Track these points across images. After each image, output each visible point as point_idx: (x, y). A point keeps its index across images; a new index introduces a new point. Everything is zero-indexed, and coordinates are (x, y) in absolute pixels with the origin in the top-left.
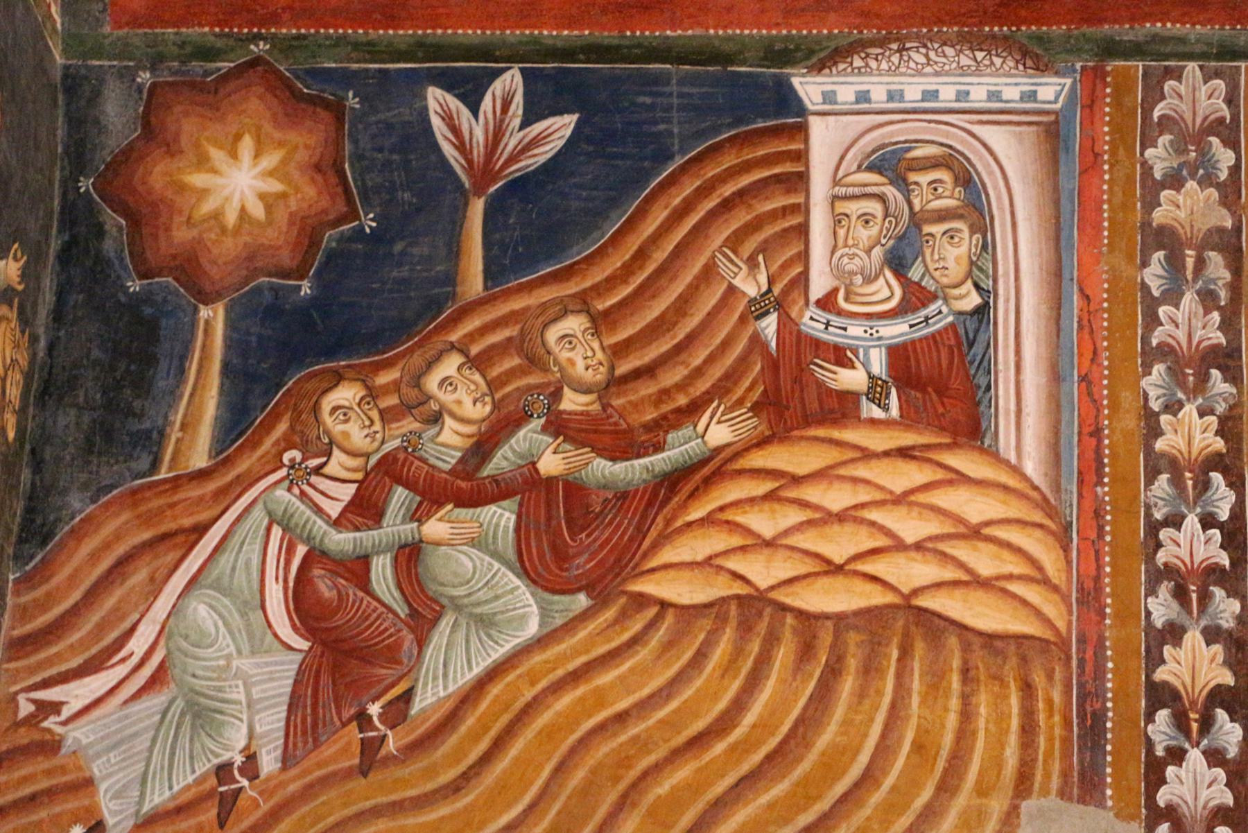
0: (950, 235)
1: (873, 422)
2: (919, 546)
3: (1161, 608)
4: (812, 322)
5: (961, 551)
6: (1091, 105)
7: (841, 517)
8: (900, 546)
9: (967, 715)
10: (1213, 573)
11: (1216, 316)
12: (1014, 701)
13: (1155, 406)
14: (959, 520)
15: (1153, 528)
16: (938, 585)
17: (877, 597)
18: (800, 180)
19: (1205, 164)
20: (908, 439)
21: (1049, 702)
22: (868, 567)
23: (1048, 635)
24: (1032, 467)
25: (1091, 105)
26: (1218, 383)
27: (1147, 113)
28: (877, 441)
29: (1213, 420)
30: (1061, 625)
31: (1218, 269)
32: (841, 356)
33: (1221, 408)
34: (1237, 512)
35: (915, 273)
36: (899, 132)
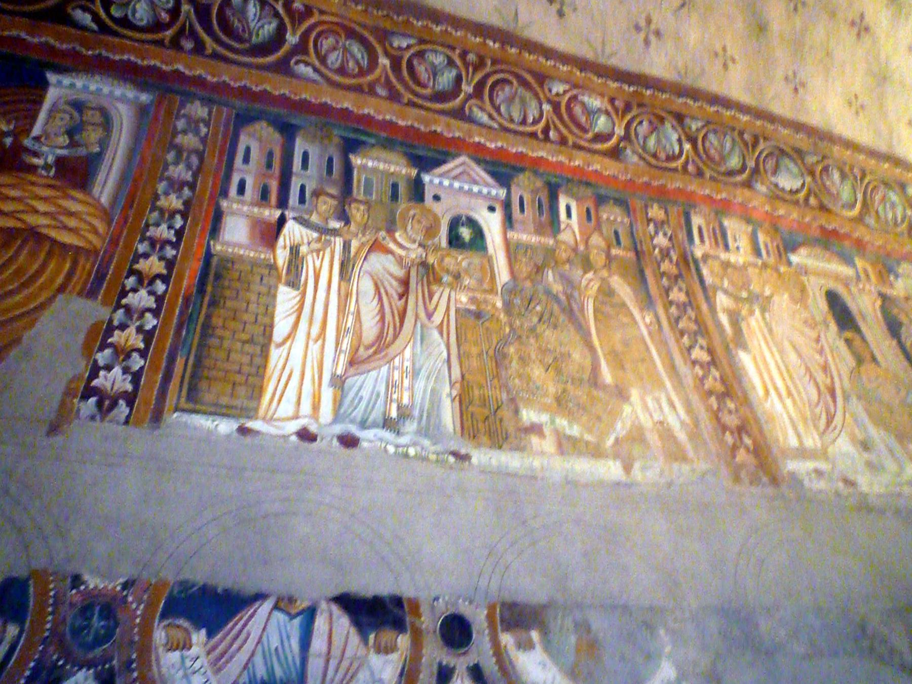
0: (94, 130)
1: (42, 176)
2: (45, 214)
3: (142, 248)
4: (27, 142)
5: (64, 219)
6: (159, 104)
7: (14, 199)
8: (36, 211)
9: (44, 266)
10: (169, 242)
11: (190, 173)
12: (67, 266)
13: (159, 192)
14: (66, 209)
15: (147, 226)
16: (48, 226)
17: (19, 225)
18: (39, 102)
19: (197, 132)
20: (52, 182)
21: (84, 269)
22: (18, 215)
23: (88, 246)
24: (105, 200)
25: (159, 104)
26: (186, 192)
27: (179, 111)
28: (43, 181)
29: (181, 201)
30: (99, 247)
31: (195, 161)
32: (36, 154)
33: (185, 198)
34: (183, 228)
35: (77, 138)
36: (82, 97)
